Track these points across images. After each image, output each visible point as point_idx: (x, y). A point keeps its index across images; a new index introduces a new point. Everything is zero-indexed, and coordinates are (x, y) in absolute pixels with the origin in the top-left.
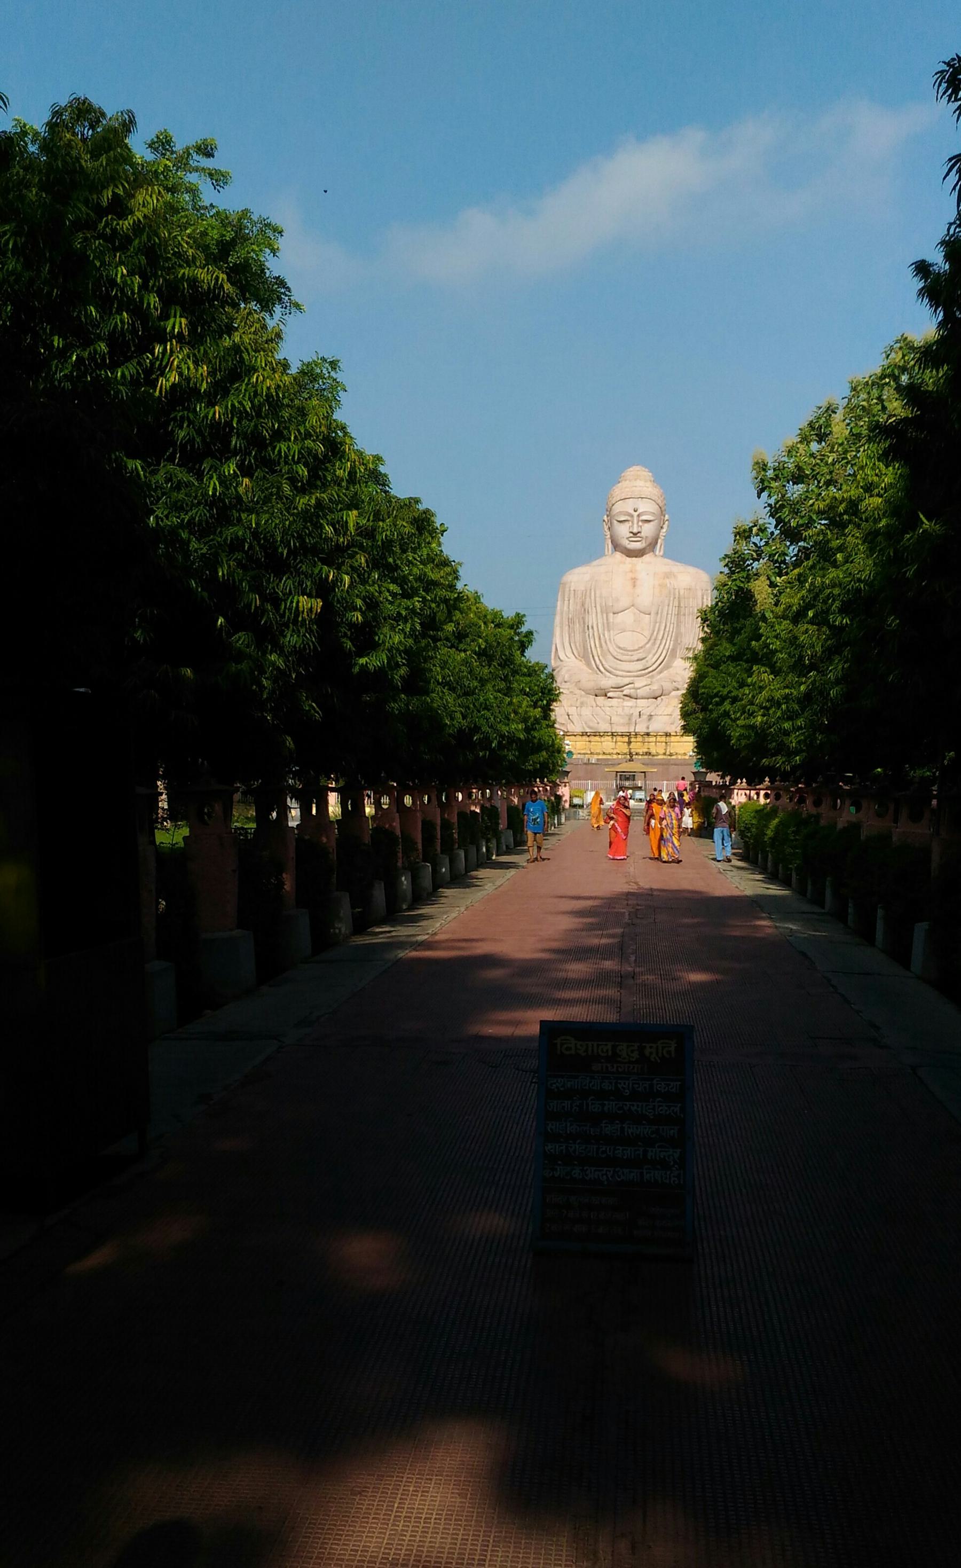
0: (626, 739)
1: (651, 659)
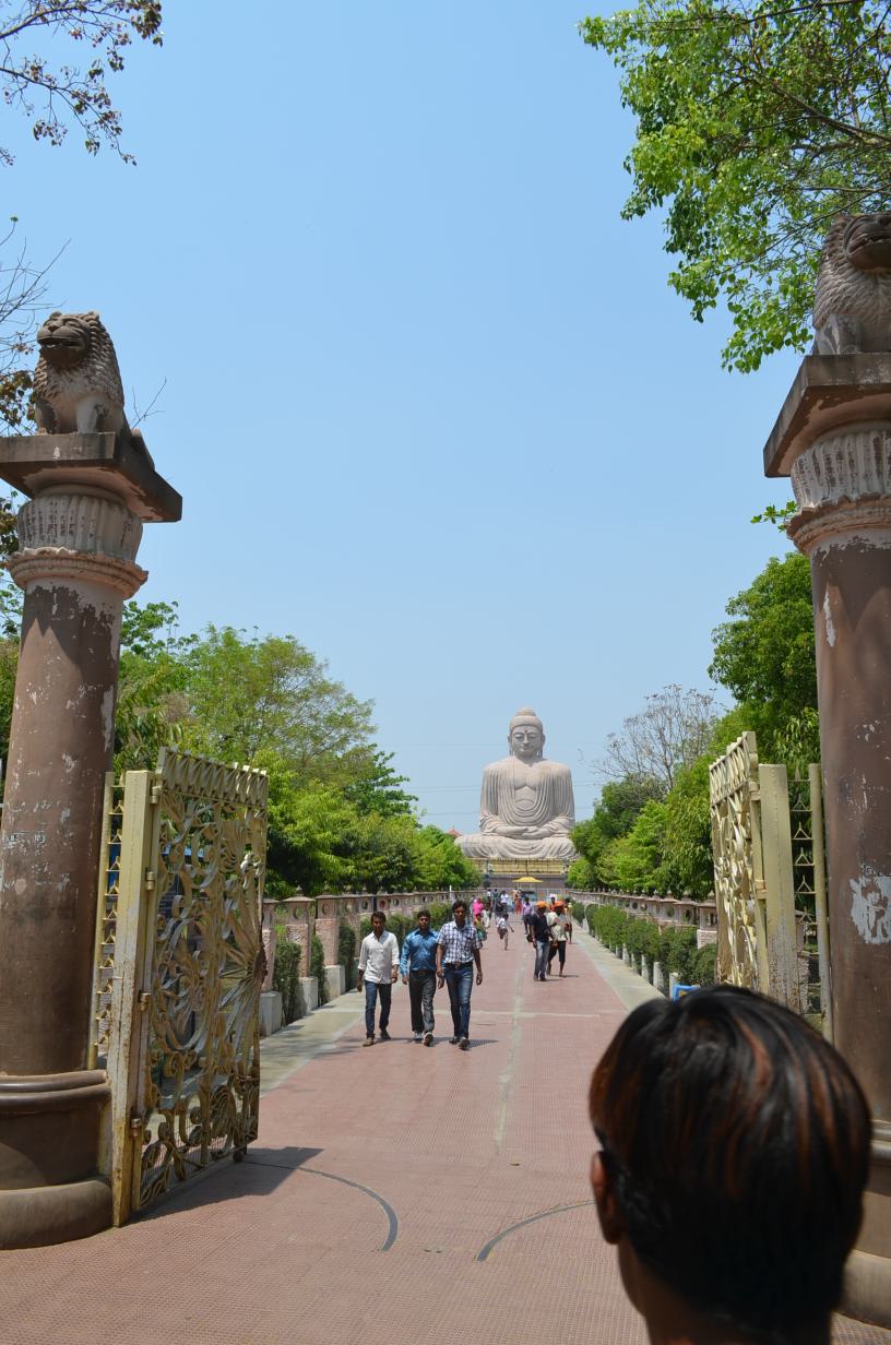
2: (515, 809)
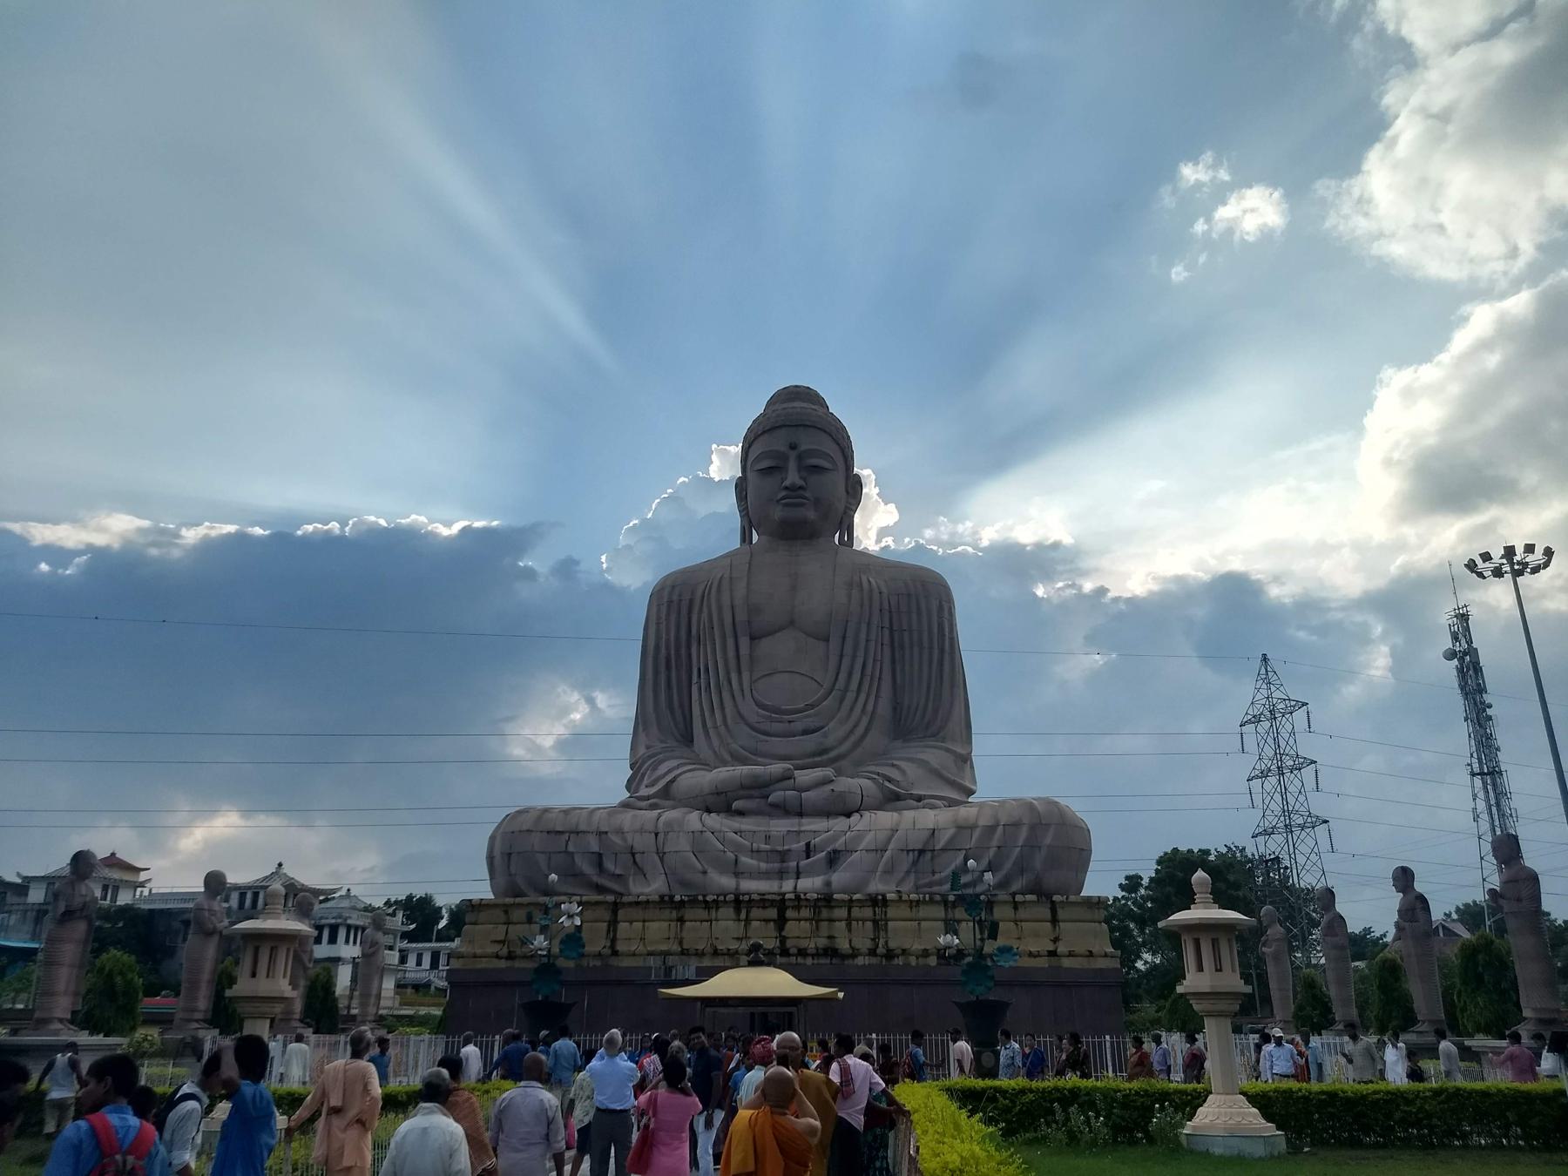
0: (772, 913)
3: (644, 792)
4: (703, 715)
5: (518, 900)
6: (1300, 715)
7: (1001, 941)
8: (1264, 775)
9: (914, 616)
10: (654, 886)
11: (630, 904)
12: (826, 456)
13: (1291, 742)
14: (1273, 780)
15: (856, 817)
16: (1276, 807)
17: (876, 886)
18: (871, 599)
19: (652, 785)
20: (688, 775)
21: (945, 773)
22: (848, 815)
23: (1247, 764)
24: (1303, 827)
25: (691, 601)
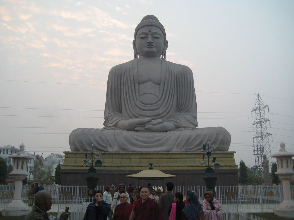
1: (161, 110)
2: (138, 103)
3: (109, 125)
4: (125, 105)
5: (78, 152)
6: (266, 109)
7: (216, 163)
8: (257, 123)
9: (183, 79)
10: (115, 149)
11: (109, 154)
12: (159, 34)
13: (264, 115)
14: (259, 125)
15: (168, 132)
16: (259, 131)
17: (175, 150)
18: (172, 74)
19: (112, 123)
20: (122, 121)
21: (191, 121)
22: (166, 132)
23: (253, 120)
24: (265, 136)
25: (121, 74)
